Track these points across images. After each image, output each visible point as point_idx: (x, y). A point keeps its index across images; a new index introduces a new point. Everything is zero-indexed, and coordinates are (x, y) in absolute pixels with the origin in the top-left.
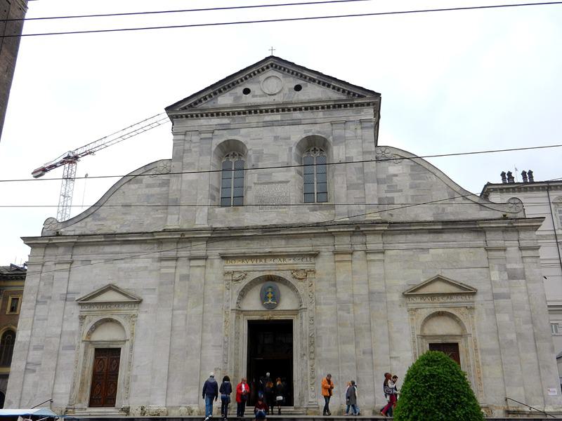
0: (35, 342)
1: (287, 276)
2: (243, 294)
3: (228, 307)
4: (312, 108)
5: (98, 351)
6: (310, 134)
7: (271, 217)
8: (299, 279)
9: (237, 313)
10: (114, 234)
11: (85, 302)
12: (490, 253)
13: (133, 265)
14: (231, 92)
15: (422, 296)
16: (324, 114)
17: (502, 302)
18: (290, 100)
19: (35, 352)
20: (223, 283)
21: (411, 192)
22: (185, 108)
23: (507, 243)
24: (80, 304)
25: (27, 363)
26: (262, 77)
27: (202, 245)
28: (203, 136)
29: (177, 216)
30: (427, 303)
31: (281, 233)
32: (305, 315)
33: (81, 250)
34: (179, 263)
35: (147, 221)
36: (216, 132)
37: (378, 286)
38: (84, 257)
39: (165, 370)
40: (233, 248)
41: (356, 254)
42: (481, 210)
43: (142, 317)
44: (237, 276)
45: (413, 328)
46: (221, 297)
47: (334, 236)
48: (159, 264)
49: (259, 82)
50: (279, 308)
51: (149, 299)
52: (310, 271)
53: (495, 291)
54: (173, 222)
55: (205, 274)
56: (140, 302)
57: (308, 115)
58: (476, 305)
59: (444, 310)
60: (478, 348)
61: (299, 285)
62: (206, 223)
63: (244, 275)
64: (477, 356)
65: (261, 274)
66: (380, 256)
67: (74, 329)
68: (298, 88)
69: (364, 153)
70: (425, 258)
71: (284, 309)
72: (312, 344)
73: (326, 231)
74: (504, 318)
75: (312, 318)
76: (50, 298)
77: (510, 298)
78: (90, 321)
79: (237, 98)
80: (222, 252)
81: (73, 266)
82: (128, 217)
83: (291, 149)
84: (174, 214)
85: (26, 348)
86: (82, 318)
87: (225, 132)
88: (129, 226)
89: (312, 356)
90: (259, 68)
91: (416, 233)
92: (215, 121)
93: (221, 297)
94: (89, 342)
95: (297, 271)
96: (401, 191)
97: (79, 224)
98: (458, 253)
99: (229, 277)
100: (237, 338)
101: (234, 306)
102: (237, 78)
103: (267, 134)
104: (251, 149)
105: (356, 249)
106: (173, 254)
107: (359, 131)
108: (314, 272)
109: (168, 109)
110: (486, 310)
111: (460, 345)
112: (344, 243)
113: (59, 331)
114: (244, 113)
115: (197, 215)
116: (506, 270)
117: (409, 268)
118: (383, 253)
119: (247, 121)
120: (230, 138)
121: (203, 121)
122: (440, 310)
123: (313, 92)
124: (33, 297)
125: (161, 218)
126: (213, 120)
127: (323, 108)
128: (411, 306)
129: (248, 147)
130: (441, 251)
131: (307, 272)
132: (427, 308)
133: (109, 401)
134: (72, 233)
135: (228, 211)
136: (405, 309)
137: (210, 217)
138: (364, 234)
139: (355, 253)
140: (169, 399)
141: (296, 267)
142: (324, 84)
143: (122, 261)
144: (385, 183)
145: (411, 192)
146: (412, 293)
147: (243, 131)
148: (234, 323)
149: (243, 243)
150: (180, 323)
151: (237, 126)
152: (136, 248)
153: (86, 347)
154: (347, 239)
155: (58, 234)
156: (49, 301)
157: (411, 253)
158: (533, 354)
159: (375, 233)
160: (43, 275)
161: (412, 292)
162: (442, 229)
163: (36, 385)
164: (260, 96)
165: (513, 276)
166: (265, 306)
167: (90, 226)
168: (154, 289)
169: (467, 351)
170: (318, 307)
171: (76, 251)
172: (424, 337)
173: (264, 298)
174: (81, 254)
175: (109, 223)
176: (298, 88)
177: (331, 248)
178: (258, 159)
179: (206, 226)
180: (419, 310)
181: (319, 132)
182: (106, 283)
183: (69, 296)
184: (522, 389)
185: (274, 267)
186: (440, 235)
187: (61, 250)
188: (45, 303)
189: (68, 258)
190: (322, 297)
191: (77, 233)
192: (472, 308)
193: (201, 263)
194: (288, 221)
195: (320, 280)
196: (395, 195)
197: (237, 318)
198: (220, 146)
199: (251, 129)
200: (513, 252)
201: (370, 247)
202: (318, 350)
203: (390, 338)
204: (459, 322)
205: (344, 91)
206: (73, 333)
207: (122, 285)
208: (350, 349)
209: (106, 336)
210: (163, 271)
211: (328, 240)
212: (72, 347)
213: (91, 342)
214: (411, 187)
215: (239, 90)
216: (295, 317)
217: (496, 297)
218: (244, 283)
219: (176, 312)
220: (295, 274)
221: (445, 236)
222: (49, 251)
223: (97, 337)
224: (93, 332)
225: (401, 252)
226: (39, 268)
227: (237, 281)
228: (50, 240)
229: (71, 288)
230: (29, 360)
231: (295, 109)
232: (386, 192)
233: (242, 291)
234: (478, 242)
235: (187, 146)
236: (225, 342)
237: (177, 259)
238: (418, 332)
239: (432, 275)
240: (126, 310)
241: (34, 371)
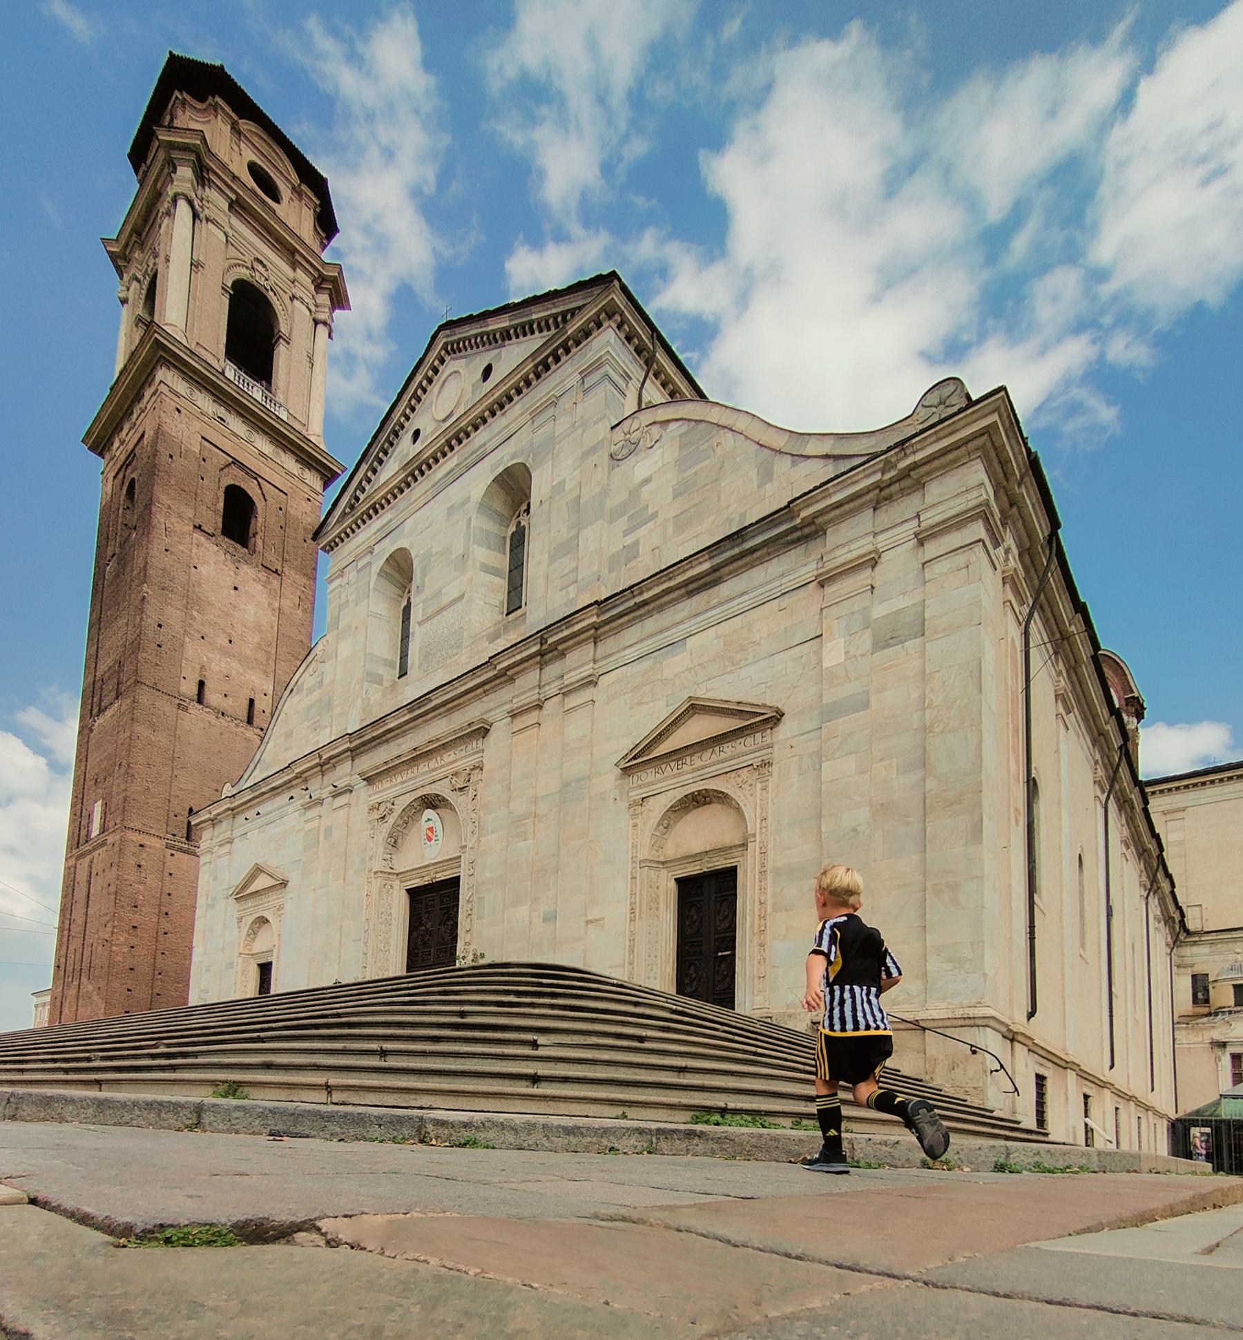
15: (676, 755)
28: (361, 564)
92: (376, 524)
132: (671, 784)
139: (547, 705)
146: (638, 761)
161: (634, 758)
162: (715, 569)
186: (710, 591)
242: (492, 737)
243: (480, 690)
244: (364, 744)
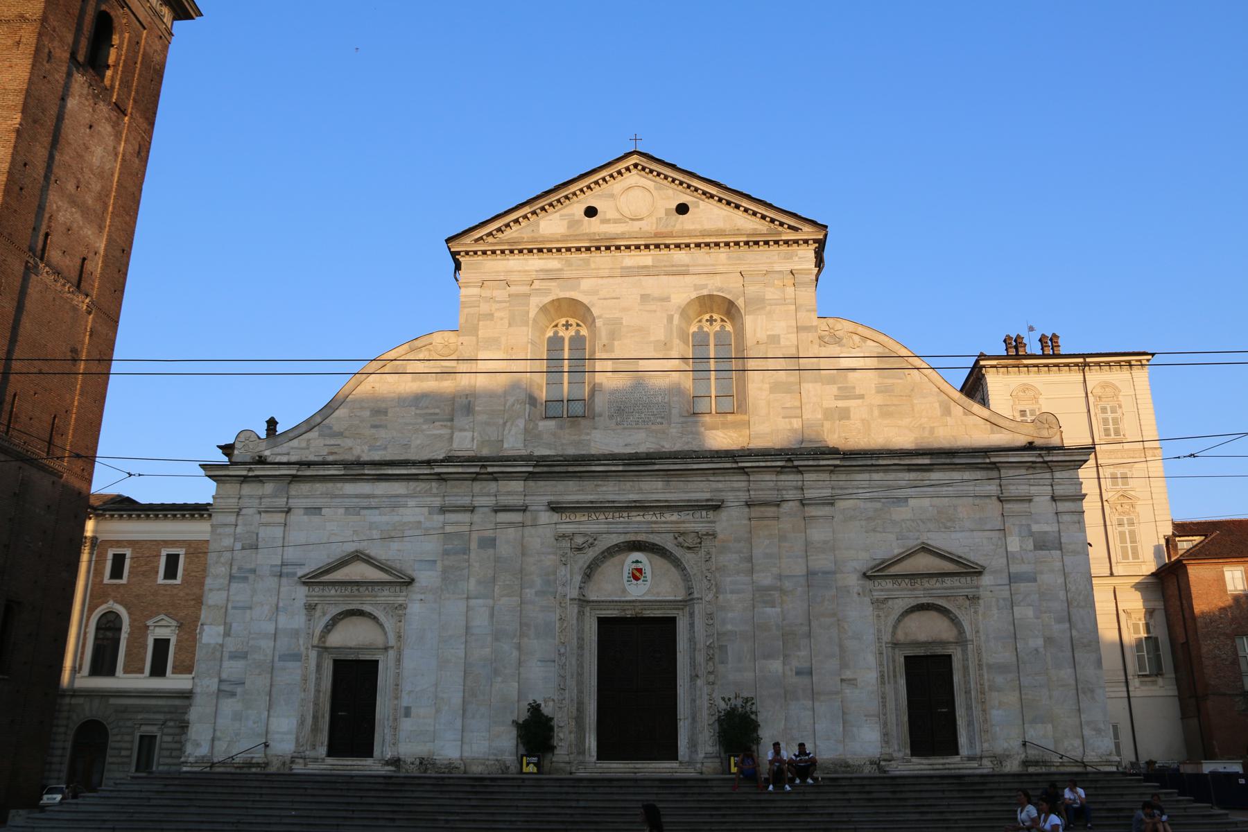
0: (232, 645)
4: (707, 245)
5: (338, 664)
6: (705, 292)
7: (640, 441)
8: (689, 548)
9: (580, 606)
10: (360, 464)
11: (311, 581)
12: (1007, 506)
13: (397, 518)
14: (561, 212)
16: (729, 258)
17: (1023, 587)
18: (669, 229)
19: (233, 663)
20: (555, 554)
21: (878, 400)
22: (481, 238)
23: (1034, 490)
24: (305, 583)
25: (221, 681)
26: (617, 186)
27: (517, 486)
28: (513, 289)
29: (469, 434)
30: (902, 590)
33: (305, 488)
34: (477, 517)
35: (417, 441)
36: (537, 284)
37: (821, 562)
38: (309, 503)
39: (457, 699)
40: (571, 492)
41: (785, 507)
42: (993, 432)
43: (416, 608)
44: (579, 540)
45: (879, 631)
46: (552, 577)
47: (747, 474)
48: (441, 518)
49: (612, 196)
51: (426, 578)
52: (707, 534)
53: (1014, 569)
54: (466, 442)
56: (411, 581)
57: (701, 255)
58: (982, 592)
59: (930, 601)
60: (984, 661)
61: (688, 558)
62: (520, 445)
64: (981, 676)
65: (622, 539)
66: (826, 510)
67: (297, 627)
68: (682, 209)
69: (799, 329)
70: (901, 513)
73: (734, 465)
74: (1024, 612)
76: (254, 571)
77: (1035, 580)
78: (324, 614)
79: (573, 223)
80: (552, 498)
81: (293, 518)
82: (382, 433)
83: (670, 318)
84: (465, 430)
85: (218, 654)
86: (310, 608)
87: (553, 284)
88: (385, 448)
89: (711, 678)
90: (613, 170)
91: (885, 471)
92: (535, 263)
93: (552, 577)
94: (323, 649)
95: (682, 534)
96: (861, 397)
97: (295, 443)
98: (955, 507)
99: (566, 544)
100: (581, 647)
101: (574, 593)
102: (575, 188)
103: (629, 290)
104: (600, 317)
105: (787, 497)
106: (466, 501)
107: (790, 290)
108: (714, 535)
109: (448, 241)
110: (998, 601)
111: (955, 659)
112: (765, 486)
113: (270, 628)
114: (588, 249)
115: (506, 432)
116: (1031, 534)
117: (874, 530)
118: (832, 504)
119: (593, 266)
120: (562, 295)
121: (515, 263)
122: (924, 601)
123: (710, 216)
124: (222, 570)
125: (440, 436)
126: (531, 262)
127: (727, 244)
128: (876, 594)
129: (595, 312)
130: (926, 502)
132: (904, 597)
133: (366, 749)
134: (284, 459)
135: (561, 428)
136: (867, 600)
137: (530, 434)
138: (798, 470)
140: (466, 747)
141: (683, 527)
142: (729, 203)
143: (377, 512)
144: (834, 383)
145: (878, 400)
146: (877, 573)
147: (586, 284)
148: (575, 622)
149: (588, 485)
150: (481, 621)
151: (574, 274)
152: (398, 488)
153: (320, 656)
155: (261, 461)
156: (252, 577)
157: (878, 505)
158: (1070, 671)
159: (818, 469)
160: (239, 530)
163: (237, 717)
164: (616, 221)
165: (1041, 544)
167: (314, 447)
168: (435, 561)
169: (966, 669)
171: (296, 489)
172: (895, 645)
174: (303, 494)
175: (348, 443)
176: (682, 209)
177: (744, 496)
178: (613, 335)
179: (523, 452)
180: (890, 602)
181: (720, 290)
182: (350, 548)
183: (285, 570)
184: (1050, 726)
185: (644, 527)
187: (269, 488)
188: (245, 579)
189: (281, 502)
191: (294, 459)
192: (974, 599)
193: (516, 517)
194: (668, 446)
196: (851, 403)
198: (544, 309)
199: (600, 281)
200: (1042, 504)
201: (809, 494)
203: (841, 646)
204: (954, 621)
205: (763, 217)
206: (296, 633)
207: (377, 551)
208: (776, 666)
209: (352, 637)
210: (448, 529)
211: (739, 482)
212: (296, 657)
213: (326, 648)
214: (879, 391)
215: (578, 208)
216: (680, 613)
217: (1012, 579)
218: (591, 554)
219: (473, 602)
220: (680, 539)
221: (935, 476)
222: (247, 489)
223: (337, 638)
224: (329, 631)
225: (861, 504)
226: (232, 519)
227: (580, 549)
228: (250, 469)
229: (291, 554)
230: (224, 676)
231: (678, 246)
232: (837, 398)
233: (589, 567)
234: (989, 488)
235: (484, 308)
237: (472, 509)
238: (887, 638)
239: (913, 543)
240: (386, 595)
241: (233, 694)
242: (723, 515)
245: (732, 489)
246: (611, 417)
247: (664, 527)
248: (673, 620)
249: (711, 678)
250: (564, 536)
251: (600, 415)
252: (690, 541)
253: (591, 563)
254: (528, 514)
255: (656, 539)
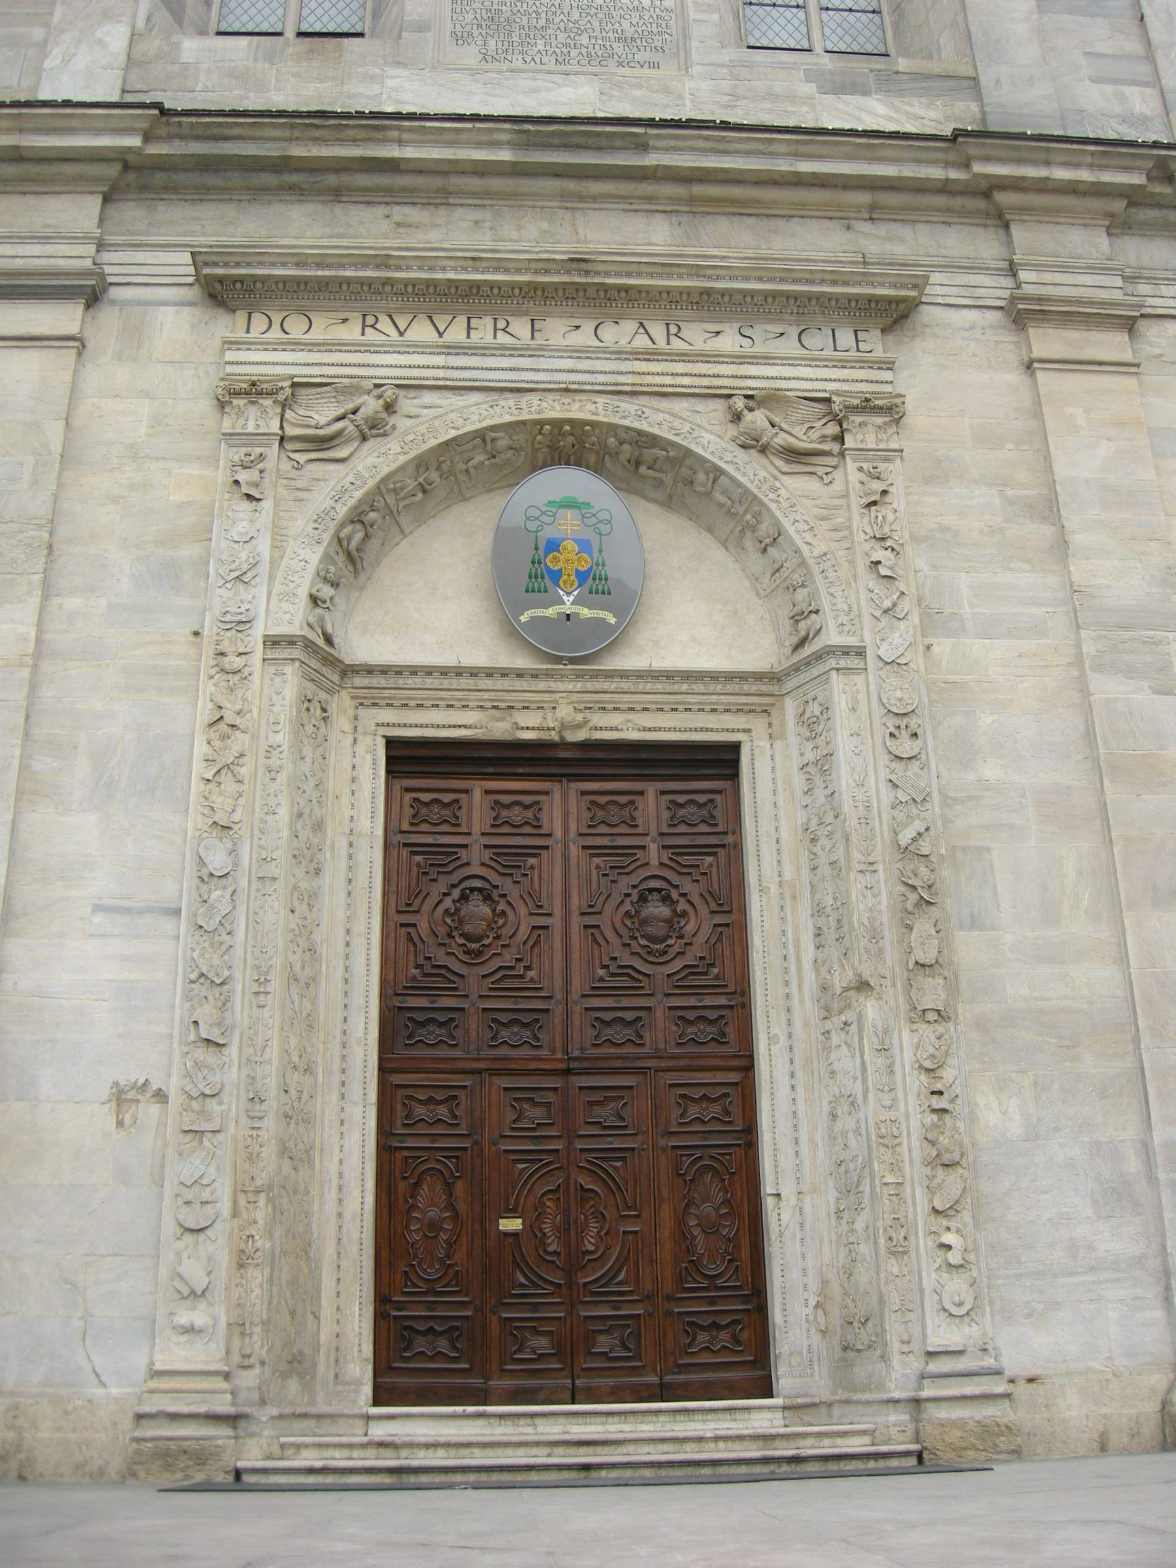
1: (705, 433)
2: (357, 547)
3: (243, 624)
8: (794, 455)
20: (212, 460)
31: (651, 160)
32: (849, 700)
44: (320, 414)
47: (1001, 221)
50: (629, 660)
52: (867, 406)
55: (74, 391)
61: (796, 502)
63: (371, 405)
65: (506, 411)
71: (659, 664)
72: (920, 899)
75: (902, 722)
89: (932, 993)
93: (188, 552)
99: (261, 419)
100: (309, 860)
101: (292, 618)
105: (1157, 305)
131: (836, 414)
141: (760, 376)
148: (283, 738)
154: (1087, 242)
166: (512, 632)
170: (942, 647)
173: (526, 573)
177: (995, 288)
185: (606, 371)
190: (963, 581)
195: (937, 473)
197: (314, 712)
202: (969, 949)
216: (758, 725)
233: (357, 517)
236: (208, 878)
243: (864, 198)
244: (206, 164)
245: (952, 261)
246: (461, 39)
247: (679, 374)
248: (721, 761)
249: (932, 993)
250: (254, 391)
251: (422, 27)
252: (802, 432)
253: (369, 503)
254: (107, 316)
255: (655, 419)
